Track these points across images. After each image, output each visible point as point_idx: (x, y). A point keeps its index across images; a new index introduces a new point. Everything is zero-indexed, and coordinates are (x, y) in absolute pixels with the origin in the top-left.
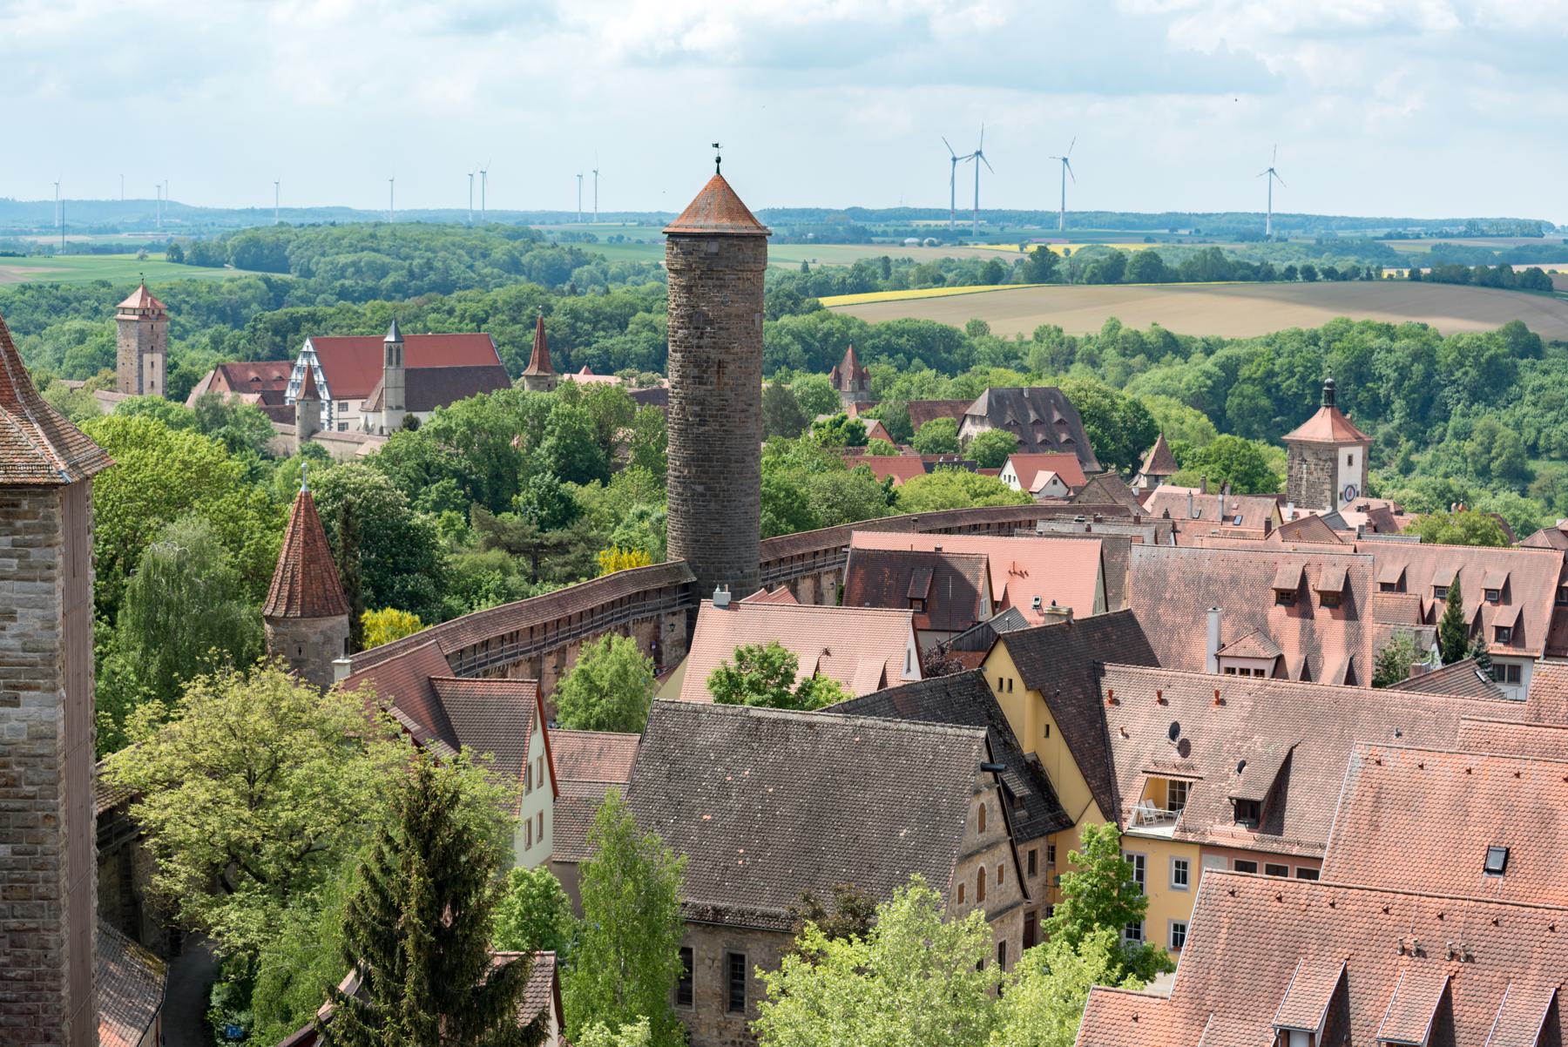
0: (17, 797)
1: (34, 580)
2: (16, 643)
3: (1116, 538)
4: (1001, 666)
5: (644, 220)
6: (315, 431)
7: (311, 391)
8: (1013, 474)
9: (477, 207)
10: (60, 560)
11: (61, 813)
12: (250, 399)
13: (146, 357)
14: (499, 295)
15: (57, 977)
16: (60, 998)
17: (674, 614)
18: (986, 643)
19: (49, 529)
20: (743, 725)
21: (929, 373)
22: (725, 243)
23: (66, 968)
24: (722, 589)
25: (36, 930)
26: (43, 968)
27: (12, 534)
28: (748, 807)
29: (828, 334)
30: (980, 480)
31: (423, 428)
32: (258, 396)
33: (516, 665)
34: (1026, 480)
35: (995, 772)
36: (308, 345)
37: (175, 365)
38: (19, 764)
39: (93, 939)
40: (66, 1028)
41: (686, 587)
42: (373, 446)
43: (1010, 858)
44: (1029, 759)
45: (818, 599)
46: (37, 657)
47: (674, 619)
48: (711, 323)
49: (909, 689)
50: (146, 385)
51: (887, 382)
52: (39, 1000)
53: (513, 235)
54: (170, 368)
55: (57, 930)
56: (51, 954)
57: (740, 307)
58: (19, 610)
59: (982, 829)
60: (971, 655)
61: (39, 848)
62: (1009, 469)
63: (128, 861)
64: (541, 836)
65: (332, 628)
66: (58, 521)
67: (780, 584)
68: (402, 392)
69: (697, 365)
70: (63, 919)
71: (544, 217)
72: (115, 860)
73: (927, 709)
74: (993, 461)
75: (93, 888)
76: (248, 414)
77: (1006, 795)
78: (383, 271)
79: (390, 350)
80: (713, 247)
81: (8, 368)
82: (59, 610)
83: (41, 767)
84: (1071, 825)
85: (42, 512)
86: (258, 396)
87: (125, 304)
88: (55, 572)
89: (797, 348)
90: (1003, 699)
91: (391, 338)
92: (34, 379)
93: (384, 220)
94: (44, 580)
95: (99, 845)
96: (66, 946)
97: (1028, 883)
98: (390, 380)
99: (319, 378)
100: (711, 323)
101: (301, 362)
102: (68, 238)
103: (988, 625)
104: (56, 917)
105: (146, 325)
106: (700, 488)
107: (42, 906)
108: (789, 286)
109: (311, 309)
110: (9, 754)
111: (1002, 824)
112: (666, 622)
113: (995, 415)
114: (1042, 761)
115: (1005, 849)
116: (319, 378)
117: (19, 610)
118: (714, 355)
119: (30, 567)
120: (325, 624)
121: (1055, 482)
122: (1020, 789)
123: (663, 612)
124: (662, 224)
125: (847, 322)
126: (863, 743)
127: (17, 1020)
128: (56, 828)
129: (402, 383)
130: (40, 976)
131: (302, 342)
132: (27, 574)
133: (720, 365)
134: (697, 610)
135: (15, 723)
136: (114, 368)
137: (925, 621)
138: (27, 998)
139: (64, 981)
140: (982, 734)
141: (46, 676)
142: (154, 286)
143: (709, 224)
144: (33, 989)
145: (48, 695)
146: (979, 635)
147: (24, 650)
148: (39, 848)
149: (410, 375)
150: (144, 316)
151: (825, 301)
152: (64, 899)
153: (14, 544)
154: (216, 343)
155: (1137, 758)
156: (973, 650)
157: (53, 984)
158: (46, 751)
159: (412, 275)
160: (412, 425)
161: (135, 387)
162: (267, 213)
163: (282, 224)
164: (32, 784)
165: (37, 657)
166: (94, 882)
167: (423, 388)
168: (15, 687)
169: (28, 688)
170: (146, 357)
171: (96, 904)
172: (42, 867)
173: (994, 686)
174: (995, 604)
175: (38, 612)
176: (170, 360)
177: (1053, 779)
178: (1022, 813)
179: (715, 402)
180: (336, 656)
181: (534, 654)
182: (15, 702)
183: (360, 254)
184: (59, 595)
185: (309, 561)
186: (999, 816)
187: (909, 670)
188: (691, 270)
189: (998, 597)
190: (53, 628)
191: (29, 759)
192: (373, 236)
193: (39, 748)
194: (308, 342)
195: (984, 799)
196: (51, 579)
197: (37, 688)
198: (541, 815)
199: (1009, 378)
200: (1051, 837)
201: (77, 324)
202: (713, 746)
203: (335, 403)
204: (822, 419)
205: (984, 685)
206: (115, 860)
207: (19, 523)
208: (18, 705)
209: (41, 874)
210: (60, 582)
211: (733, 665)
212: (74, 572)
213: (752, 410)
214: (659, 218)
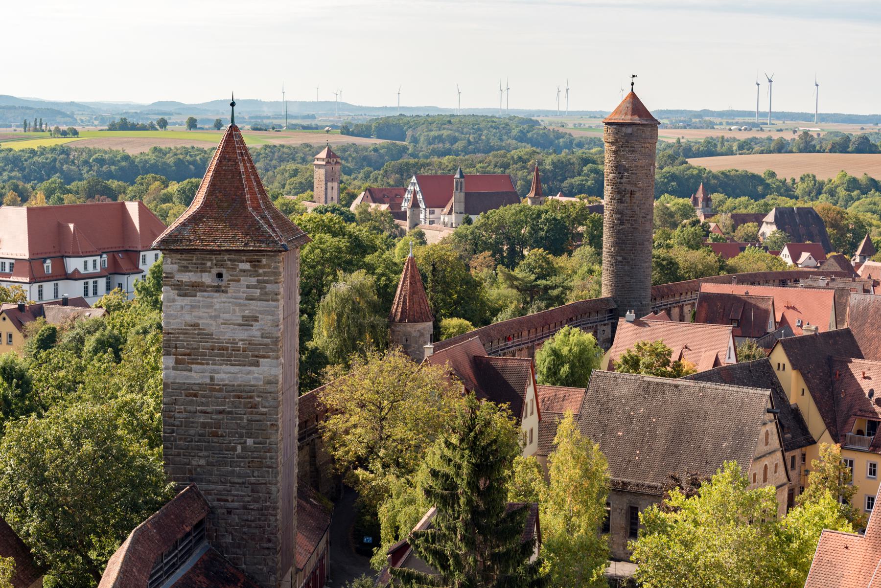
0: (257, 413)
1: (268, 301)
2: (258, 334)
3: (843, 289)
4: (779, 356)
5: (593, 115)
6: (417, 225)
7: (415, 205)
9: (504, 107)
10: (282, 290)
11: (280, 424)
12: (384, 207)
13: (329, 184)
14: (515, 153)
15: (275, 508)
16: (276, 520)
17: (605, 325)
19: (277, 274)
20: (640, 386)
22: (635, 128)
23: (280, 504)
24: (631, 312)
25: (265, 484)
26: (268, 504)
27: (258, 276)
28: (642, 429)
31: (474, 224)
32: (387, 205)
33: (521, 350)
34: (795, 257)
35: (774, 414)
36: (414, 179)
37: (345, 188)
38: (258, 396)
39: (295, 489)
40: (279, 536)
41: (611, 311)
42: (448, 232)
43: (781, 460)
44: (793, 407)
45: (682, 319)
46: (268, 341)
47: (604, 328)
48: (627, 170)
49: (730, 369)
50: (329, 199)
51: (722, 202)
52: (265, 520)
53: (524, 121)
54: (341, 191)
55: (276, 484)
56: (273, 497)
57: (643, 162)
58: (260, 316)
59: (767, 444)
61: (268, 441)
63: (314, 449)
64: (531, 442)
65: (424, 328)
66: (281, 269)
68: (463, 205)
69: (619, 193)
70: (279, 478)
71: (539, 113)
72: (307, 448)
73: (739, 379)
75: (296, 462)
76: (382, 214)
78: (454, 140)
79: (457, 182)
80: (629, 130)
81: (257, 190)
82: (281, 317)
83: (270, 399)
84: (814, 442)
85: (273, 265)
86: (387, 205)
87: (317, 156)
88: (279, 297)
90: (779, 374)
91: (457, 176)
92: (270, 196)
93: (455, 114)
94: (273, 301)
95: (299, 440)
96: (280, 494)
97: (790, 473)
98: (456, 199)
99: (420, 197)
100: (627, 170)
101: (411, 188)
102: (289, 121)
104: (276, 477)
105: (329, 167)
106: (620, 258)
107: (268, 472)
108: (670, 152)
109: (416, 160)
110: (253, 392)
111: (778, 441)
112: (601, 328)
114: (800, 408)
115: (779, 454)
116: (420, 197)
117: (260, 316)
118: (629, 188)
119: (266, 294)
120: (420, 326)
123: (598, 324)
124: (602, 117)
125: (700, 171)
127: (254, 531)
128: (277, 430)
129: (463, 199)
130: (267, 508)
131: (411, 177)
132: (266, 297)
133: (632, 193)
134: (617, 323)
135: (257, 375)
136: (312, 190)
137: (739, 331)
138: (259, 519)
139: (279, 511)
140: (768, 392)
141: (273, 351)
142: (334, 147)
143: (628, 119)
144: (263, 515)
145: (275, 361)
147: (262, 337)
148: (268, 441)
149: (467, 195)
150: (328, 163)
152: (280, 468)
153: (258, 281)
154: (367, 177)
157: (273, 512)
158: (273, 390)
159: (469, 143)
160: (469, 222)
161: (323, 200)
162: (393, 109)
163: (401, 115)
164: (265, 407)
165: (268, 341)
166: (296, 460)
167: (474, 203)
168: (257, 357)
169: (264, 357)
170: (329, 184)
171: (297, 471)
172: (269, 451)
173: (775, 368)
175: (270, 317)
176: (342, 186)
178: (788, 436)
179: (628, 212)
180: (426, 343)
181: (530, 345)
182: (257, 364)
183: (442, 132)
184: (281, 308)
185: (413, 292)
186: (776, 437)
188: (617, 142)
190: (277, 326)
191: (263, 394)
192: (450, 122)
193: (269, 388)
194: (414, 178)
196: (277, 300)
197: (268, 357)
198: (532, 430)
199: (787, 203)
200: (804, 449)
201: (291, 166)
202: (624, 396)
203: (428, 210)
205: (770, 367)
206: (307, 448)
207: (261, 271)
208: (258, 366)
209: (268, 454)
210: (282, 302)
211: (634, 352)
212: (289, 297)
213: (649, 217)
214: (601, 114)
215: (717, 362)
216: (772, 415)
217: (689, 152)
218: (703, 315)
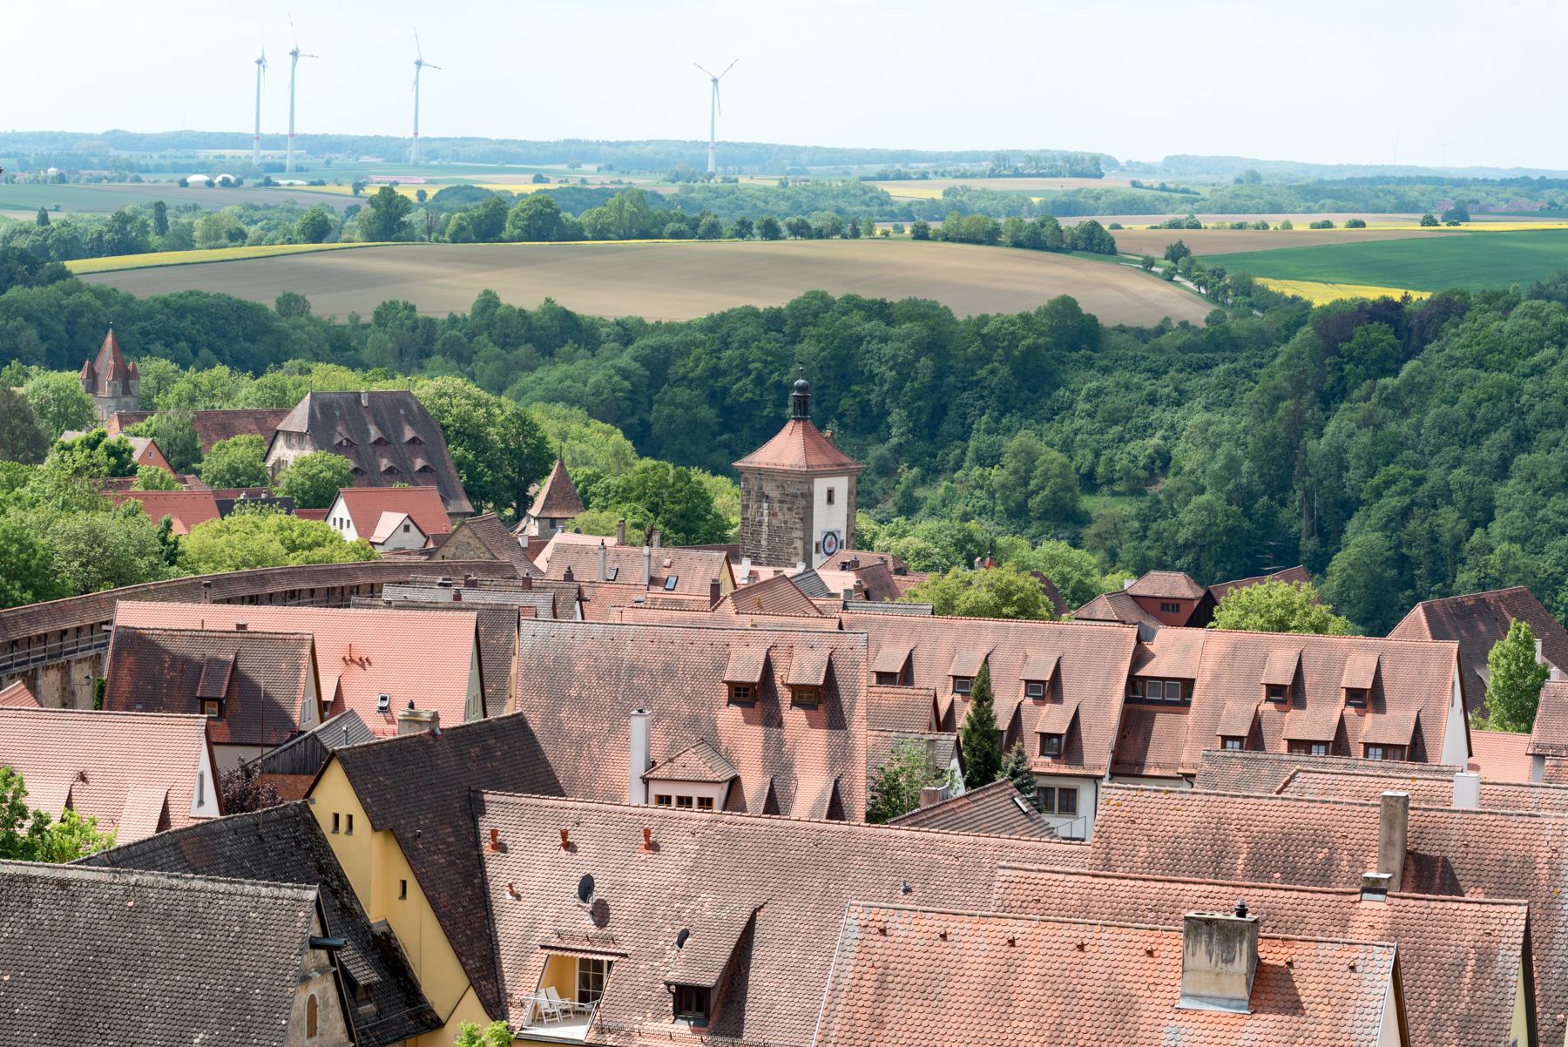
3: (497, 610)
4: (335, 796)
8: (347, 516)
18: (312, 762)
21: (221, 371)
29: (75, 314)
30: (298, 524)
34: (365, 524)
35: (331, 950)
44: (378, 930)
45: (68, 700)
49: (202, 832)
51: (162, 383)
60: (290, 779)
62: (341, 510)
67: (12, 677)
73: (230, 859)
74: (316, 499)
77: (346, 983)
84: (438, 1024)
89: (31, 333)
90: (339, 844)
103: (314, 736)
111: (341, 1025)
113: (319, 432)
121: (407, 529)
122: (364, 974)
125: (100, 294)
126: (138, 910)
140: (311, 895)
146: (300, 749)
151: (73, 265)
155: (533, 926)
156: (293, 773)
173: (326, 825)
174: (323, 706)
177: (412, 958)
178: (368, 1008)
186: (336, 1013)
187: (201, 802)
189: (328, 695)
195: (314, 989)
204: (70, 437)
205: (312, 824)
215: (164, 821)
216: (323, 954)
217: (73, 247)
218: (125, 683)
